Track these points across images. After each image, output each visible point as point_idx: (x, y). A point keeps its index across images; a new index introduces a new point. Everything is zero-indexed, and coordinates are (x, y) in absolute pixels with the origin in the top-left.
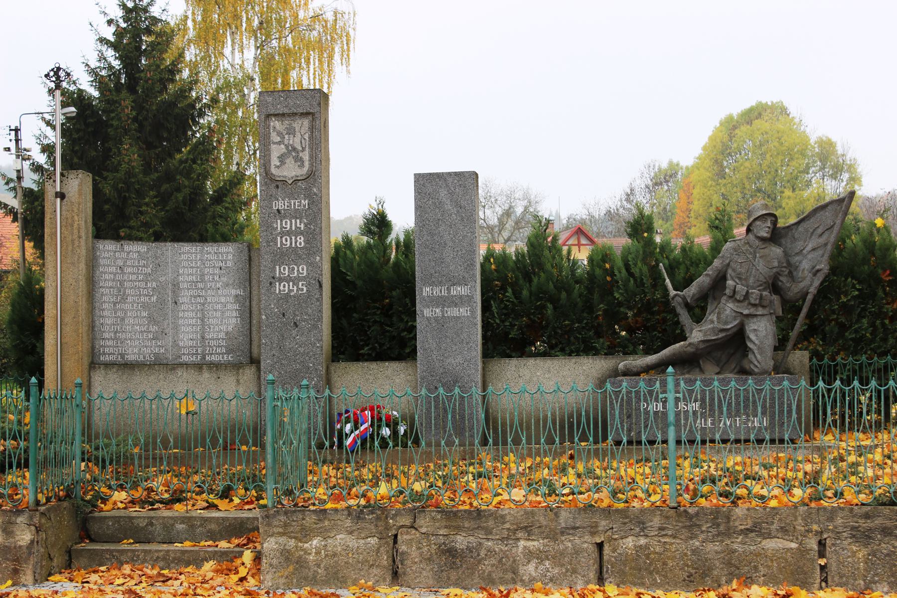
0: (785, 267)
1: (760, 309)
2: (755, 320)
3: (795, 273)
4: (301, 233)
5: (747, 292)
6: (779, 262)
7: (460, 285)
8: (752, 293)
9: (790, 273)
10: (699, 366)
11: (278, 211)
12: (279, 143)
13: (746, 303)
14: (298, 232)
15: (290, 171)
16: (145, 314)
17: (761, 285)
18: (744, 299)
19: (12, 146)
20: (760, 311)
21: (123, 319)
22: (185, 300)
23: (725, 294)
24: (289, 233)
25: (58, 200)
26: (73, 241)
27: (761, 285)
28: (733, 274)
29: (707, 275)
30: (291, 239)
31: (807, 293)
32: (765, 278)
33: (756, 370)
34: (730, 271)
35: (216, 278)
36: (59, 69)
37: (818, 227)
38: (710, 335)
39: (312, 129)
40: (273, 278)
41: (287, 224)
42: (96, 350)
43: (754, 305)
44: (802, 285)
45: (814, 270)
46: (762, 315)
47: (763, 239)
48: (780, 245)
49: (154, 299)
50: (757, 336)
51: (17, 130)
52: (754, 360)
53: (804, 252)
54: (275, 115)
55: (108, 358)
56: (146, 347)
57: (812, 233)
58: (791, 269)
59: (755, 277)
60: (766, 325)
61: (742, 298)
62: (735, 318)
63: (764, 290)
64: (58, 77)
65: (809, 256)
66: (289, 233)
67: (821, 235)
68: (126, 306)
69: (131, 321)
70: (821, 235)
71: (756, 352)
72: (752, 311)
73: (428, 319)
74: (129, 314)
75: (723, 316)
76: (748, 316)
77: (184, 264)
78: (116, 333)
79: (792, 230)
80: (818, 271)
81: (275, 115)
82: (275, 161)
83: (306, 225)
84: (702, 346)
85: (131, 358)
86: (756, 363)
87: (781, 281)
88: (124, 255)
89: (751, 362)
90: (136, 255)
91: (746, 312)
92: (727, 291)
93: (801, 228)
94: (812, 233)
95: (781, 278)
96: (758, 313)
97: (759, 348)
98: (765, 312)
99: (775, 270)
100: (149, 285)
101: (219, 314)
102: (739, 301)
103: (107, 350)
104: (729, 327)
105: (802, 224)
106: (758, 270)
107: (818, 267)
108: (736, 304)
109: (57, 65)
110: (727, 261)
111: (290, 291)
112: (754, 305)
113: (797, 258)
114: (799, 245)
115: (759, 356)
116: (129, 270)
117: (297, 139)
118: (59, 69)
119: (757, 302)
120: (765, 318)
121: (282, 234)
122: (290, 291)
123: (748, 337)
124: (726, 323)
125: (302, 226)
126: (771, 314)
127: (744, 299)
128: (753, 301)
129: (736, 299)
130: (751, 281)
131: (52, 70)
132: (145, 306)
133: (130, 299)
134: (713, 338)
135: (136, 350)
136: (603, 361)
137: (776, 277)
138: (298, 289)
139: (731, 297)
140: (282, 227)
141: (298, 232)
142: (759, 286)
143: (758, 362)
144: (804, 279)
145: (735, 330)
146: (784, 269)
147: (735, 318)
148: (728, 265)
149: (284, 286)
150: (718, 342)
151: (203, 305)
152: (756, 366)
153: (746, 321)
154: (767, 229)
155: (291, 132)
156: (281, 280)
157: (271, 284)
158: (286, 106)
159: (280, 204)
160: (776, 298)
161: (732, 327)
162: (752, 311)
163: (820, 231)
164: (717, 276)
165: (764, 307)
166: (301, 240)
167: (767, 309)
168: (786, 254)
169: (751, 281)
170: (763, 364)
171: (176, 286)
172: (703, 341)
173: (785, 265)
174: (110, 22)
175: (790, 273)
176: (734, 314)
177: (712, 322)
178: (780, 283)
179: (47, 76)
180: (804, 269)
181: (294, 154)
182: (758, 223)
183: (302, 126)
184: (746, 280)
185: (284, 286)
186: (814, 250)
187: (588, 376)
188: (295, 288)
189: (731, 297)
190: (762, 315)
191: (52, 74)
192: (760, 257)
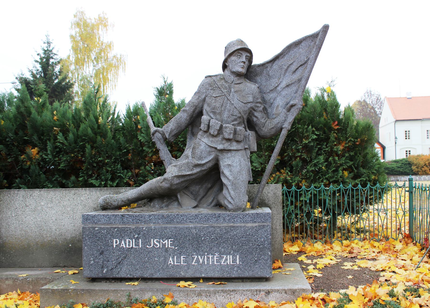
0: (260, 103)
1: (235, 144)
2: (229, 155)
3: (269, 110)
5: (221, 127)
6: (254, 97)
8: (226, 127)
9: (265, 109)
10: (177, 200)
13: (220, 138)
17: (235, 120)
18: (218, 134)
20: (235, 146)
23: (201, 129)
27: (235, 120)
28: (208, 109)
29: (184, 111)
31: (281, 129)
32: (240, 113)
33: (230, 206)
34: (206, 107)
37: (292, 64)
38: (185, 170)
43: (229, 140)
44: (276, 121)
45: (289, 105)
47: (238, 75)
48: (256, 82)
50: (231, 171)
52: (228, 196)
53: (279, 88)
57: (286, 70)
59: (229, 111)
60: (240, 161)
61: (216, 133)
62: (209, 153)
63: (239, 124)
65: (284, 93)
67: (295, 72)
70: (295, 72)
71: (230, 187)
72: (226, 145)
75: (198, 151)
76: (222, 151)
79: (267, 67)
80: (292, 106)
84: (176, 181)
86: (230, 199)
87: (256, 117)
89: (225, 198)
91: (220, 147)
92: (203, 127)
93: (275, 66)
94: (286, 70)
95: (256, 114)
96: (232, 148)
97: (233, 184)
98: (240, 147)
99: (249, 105)
102: (213, 136)
104: (203, 162)
105: (276, 62)
106: (233, 104)
107: (292, 103)
108: (211, 139)
110: (203, 97)
112: (229, 140)
113: (272, 95)
114: (274, 82)
115: (232, 193)
119: (231, 137)
120: (240, 153)
123: (223, 173)
124: (201, 158)
126: (245, 149)
127: (218, 134)
128: (227, 136)
129: (210, 134)
130: (226, 115)
136: (98, 193)
137: (251, 112)
139: (206, 132)
142: (233, 121)
143: (232, 198)
144: (278, 115)
145: (210, 165)
146: (259, 105)
147: (209, 153)
148: (204, 100)
150: (193, 177)
152: (230, 203)
153: (221, 156)
154: (242, 64)
160: (251, 134)
161: (207, 163)
162: (226, 145)
163: (293, 67)
164: (194, 111)
165: (238, 142)
167: (242, 144)
168: (261, 92)
169: (226, 115)
170: (237, 200)
172: (178, 177)
173: (259, 100)
174: (38, 54)
175: (265, 109)
176: (209, 149)
177: (187, 157)
178: (255, 119)
180: (278, 106)
182: (233, 58)
184: (220, 114)
186: (287, 86)
187: (85, 206)
189: (206, 132)
192: (235, 92)
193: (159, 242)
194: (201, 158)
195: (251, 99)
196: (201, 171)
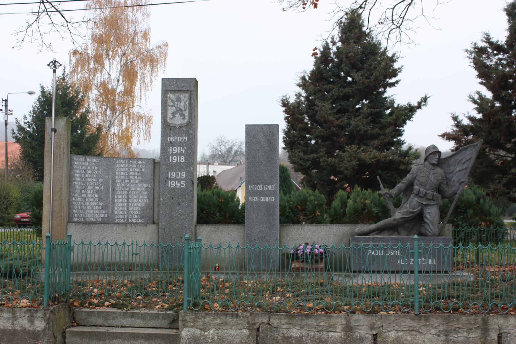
1: (432, 201)
2: (429, 207)
3: (449, 183)
4: (183, 155)
5: (426, 193)
6: (442, 177)
7: (269, 185)
8: (428, 193)
9: (447, 183)
10: (398, 231)
11: (171, 142)
12: (172, 106)
13: (425, 198)
14: (181, 154)
15: (178, 121)
16: (97, 196)
18: (424, 196)
19: (3, 108)
20: (432, 203)
21: (85, 199)
22: (118, 189)
23: (413, 193)
24: (176, 154)
25: (53, 132)
26: (60, 155)
27: (433, 189)
28: (418, 183)
29: (403, 183)
30: (177, 158)
32: (435, 185)
33: (430, 234)
34: (416, 181)
35: (136, 177)
36: (55, 61)
37: (462, 159)
38: (405, 215)
39: (190, 99)
40: (167, 178)
41: (176, 150)
42: (71, 215)
44: (454, 189)
45: (460, 182)
46: (433, 205)
47: (434, 165)
48: (441, 168)
49: (102, 188)
50: (430, 216)
51: (6, 101)
52: (428, 228)
53: (454, 172)
54: (170, 91)
55: (77, 220)
56: (97, 214)
57: (459, 162)
58: (447, 180)
59: (430, 184)
61: (423, 196)
63: (434, 191)
64: (55, 66)
65: (457, 174)
66: (176, 154)
67: (464, 163)
68: (87, 192)
69: (90, 200)
70: (464, 163)
71: (430, 224)
72: (428, 202)
73: (252, 203)
74: (88, 196)
77: (119, 169)
78: (81, 205)
79: (448, 160)
80: (462, 182)
81: (170, 91)
82: (170, 115)
83: (185, 150)
84: (401, 220)
85: (89, 219)
86: (430, 230)
87: (443, 187)
88: (87, 164)
89: (427, 229)
90: (93, 164)
91: (425, 203)
92: (415, 192)
93: (453, 160)
94: (459, 162)
95: (443, 185)
96: (431, 204)
97: (432, 223)
98: (435, 203)
99: (440, 181)
100: (100, 180)
101: (137, 197)
102: (421, 197)
103: (76, 215)
104: (415, 211)
105: (453, 157)
106: (431, 181)
107: (462, 180)
108: (420, 199)
109: (55, 60)
110: (415, 176)
111: (176, 185)
112: (429, 200)
113: (450, 175)
114: (452, 168)
115: (431, 226)
116: (89, 172)
117: (182, 104)
118: (55, 61)
119: (431, 198)
121: (173, 155)
122: (176, 185)
123: (426, 216)
124: (414, 209)
125: (184, 151)
126: (437, 204)
127: (424, 196)
128: (429, 197)
129: (419, 196)
130: (428, 187)
131: (52, 62)
132: (97, 192)
133: (89, 188)
134: (407, 216)
135: (92, 216)
136: (344, 227)
137: (440, 185)
138: (181, 185)
139: (417, 195)
140: (173, 151)
141: (181, 154)
143: (431, 230)
144: (454, 186)
145: (418, 212)
146: (444, 181)
148: (415, 178)
149: (173, 183)
150: (409, 218)
151: (128, 191)
152: (430, 232)
153: (424, 208)
155: (179, 100)
156: (171, 180)
157: (166, 181)
158: (176, 87)
159: (172, 139)
162: (428, 202)
163: (463, 161)
164: (409, 183)
165: (434, 200)
166: (183, 158)
168: (445, 173)
169: (428, 187)
170: (433, 231)
171: (114, 182)
172: (402, 218)
173: (445, 178)
175: (447, 183)
176: (418, 204)
177: (407, 208)
178: (442, 188)
179: (49, 65)
180: (454, 181)
181: (180, 112)
182: (431, 156)
183: (184, 97)
184: (425, 186)
185: (173, 183)
186: (460, 171)
187: (336, 235)
188: (179, 184)
189: (417, 195)
190: (433, 205)
191: (51, 64)
193: (393, 252)
194: (414, 209)
195: (440, 178)
196: (414, 215)
